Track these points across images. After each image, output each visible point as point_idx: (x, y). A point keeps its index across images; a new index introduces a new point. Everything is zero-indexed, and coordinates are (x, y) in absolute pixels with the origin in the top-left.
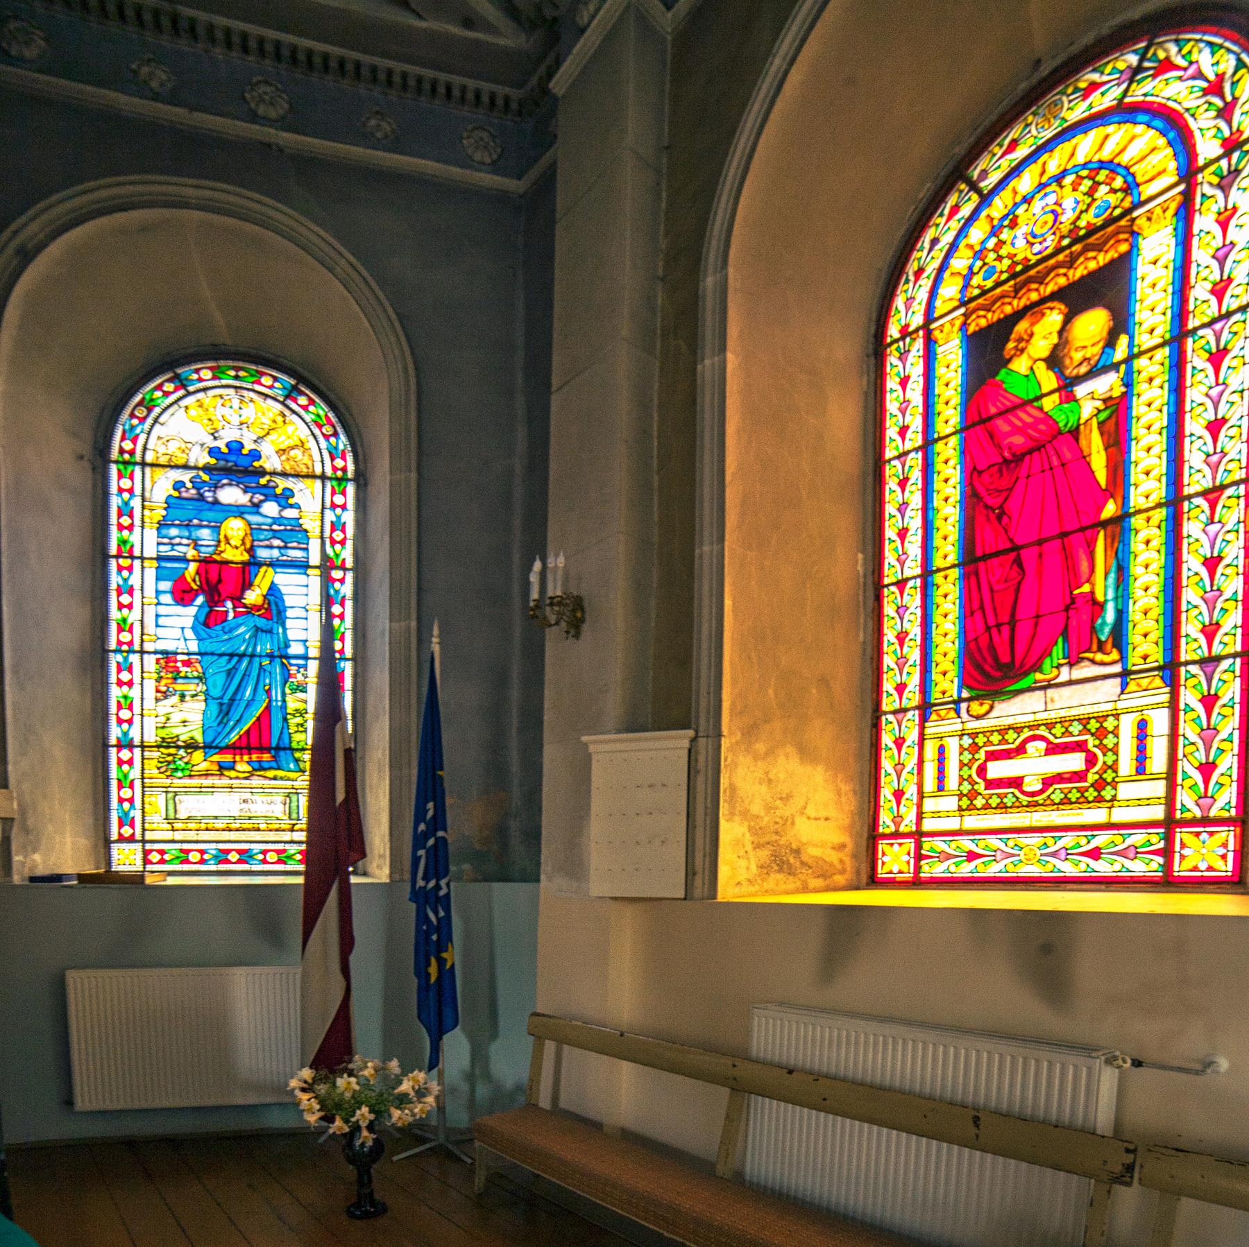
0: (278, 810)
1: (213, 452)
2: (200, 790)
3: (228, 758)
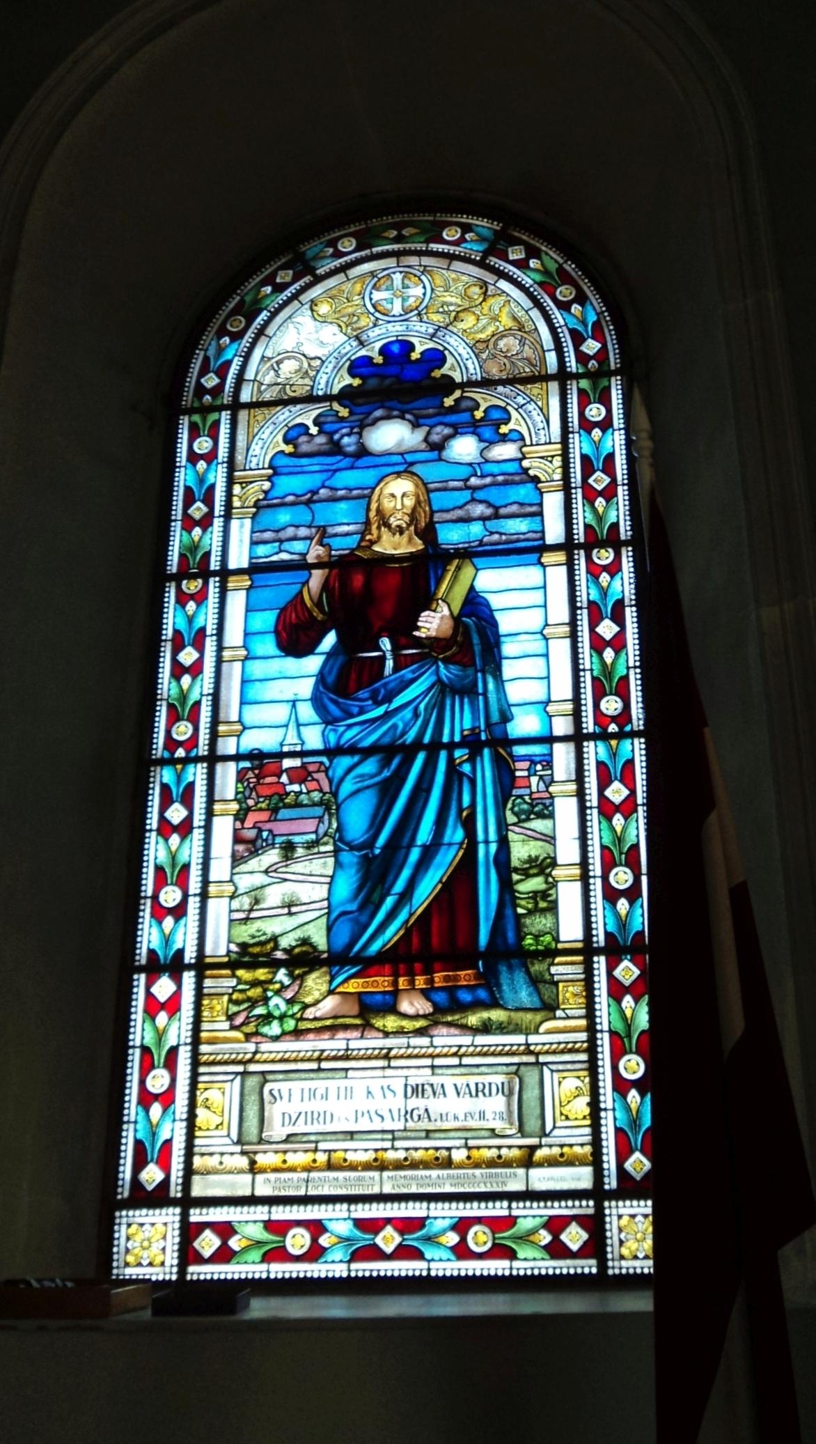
1: (356, 367)
2: (320, 1064)
3: (381, 983)
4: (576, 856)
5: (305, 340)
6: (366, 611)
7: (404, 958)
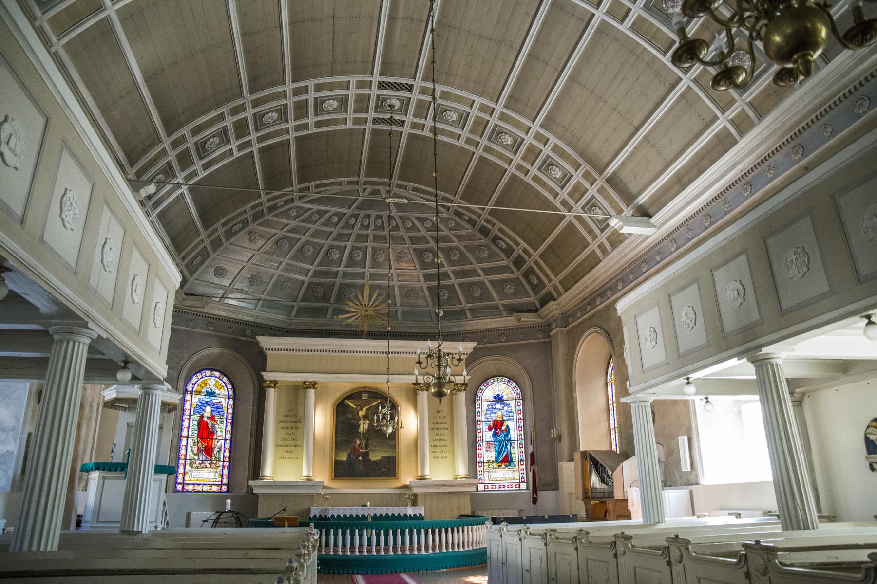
0: (511, 476)
4: (517, 452)
5: (488, 393)
6: (496, 426)
7: (502, 462)
